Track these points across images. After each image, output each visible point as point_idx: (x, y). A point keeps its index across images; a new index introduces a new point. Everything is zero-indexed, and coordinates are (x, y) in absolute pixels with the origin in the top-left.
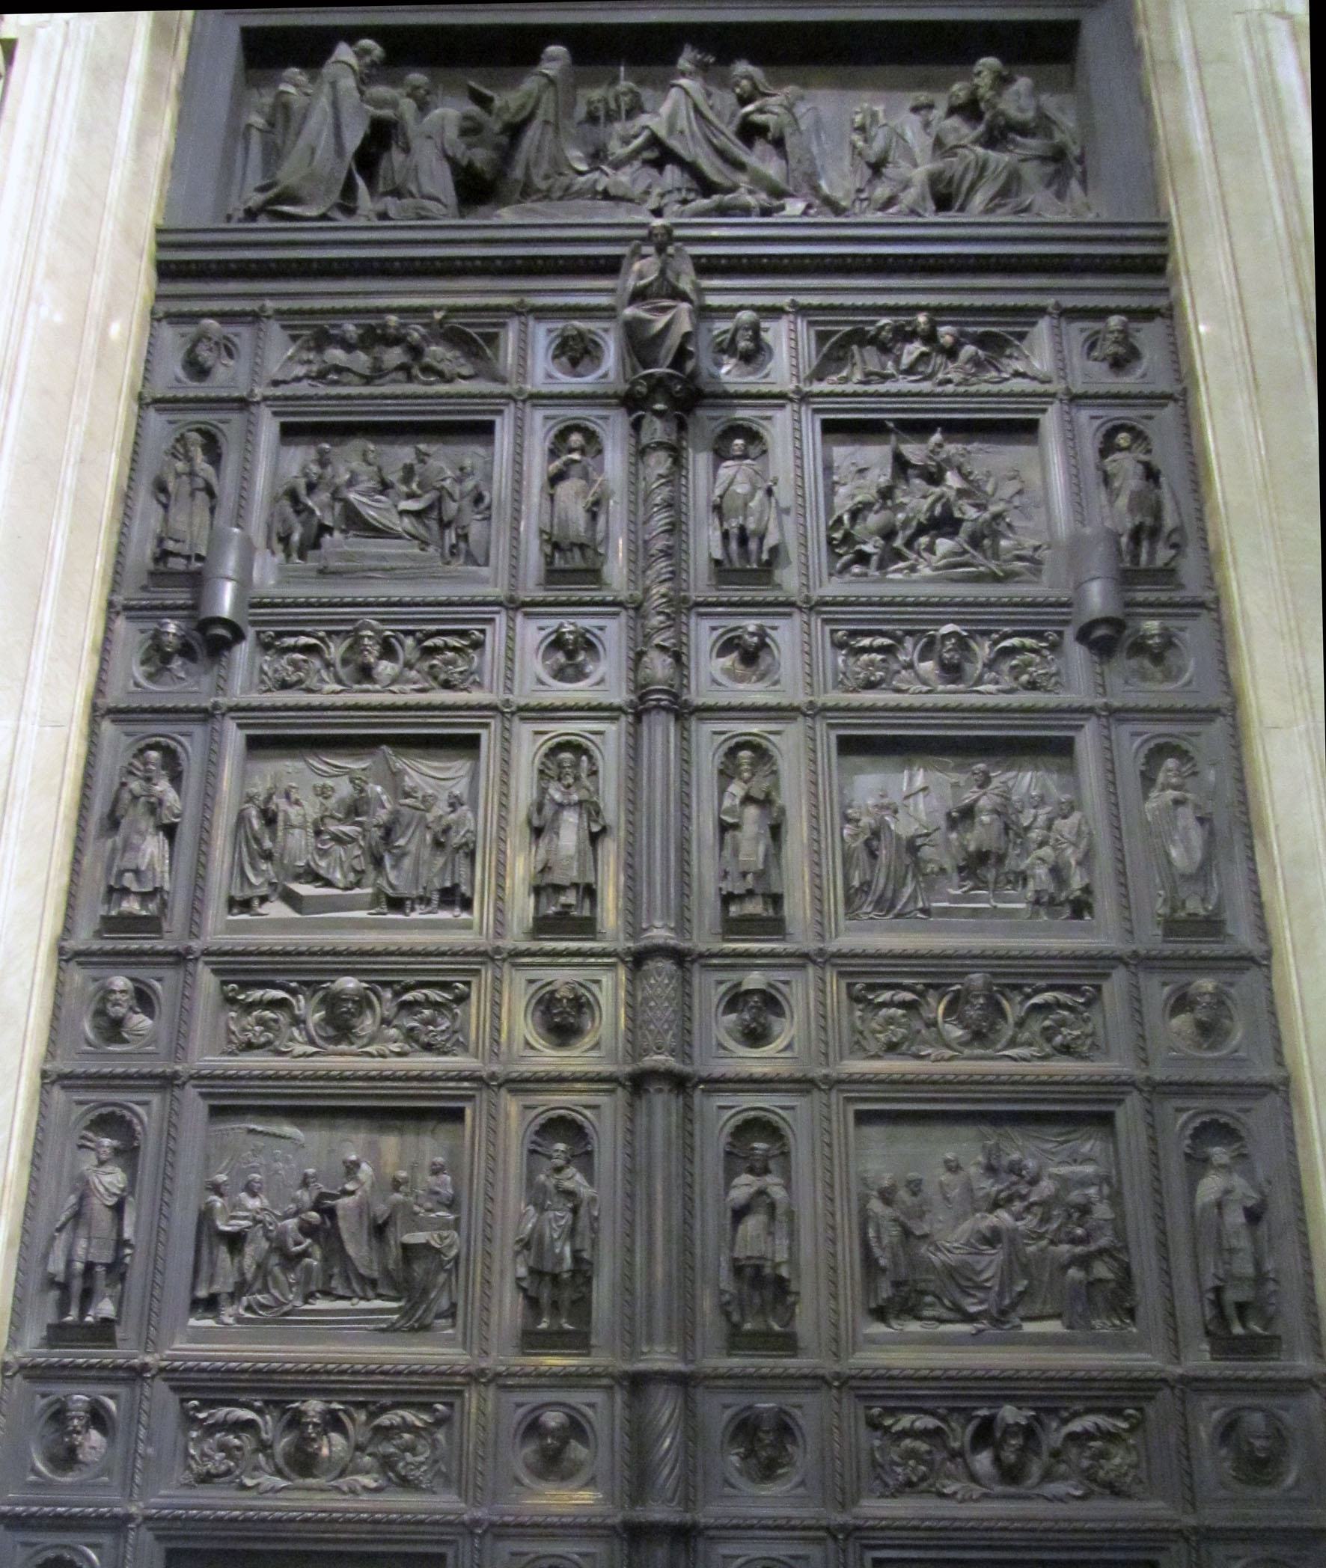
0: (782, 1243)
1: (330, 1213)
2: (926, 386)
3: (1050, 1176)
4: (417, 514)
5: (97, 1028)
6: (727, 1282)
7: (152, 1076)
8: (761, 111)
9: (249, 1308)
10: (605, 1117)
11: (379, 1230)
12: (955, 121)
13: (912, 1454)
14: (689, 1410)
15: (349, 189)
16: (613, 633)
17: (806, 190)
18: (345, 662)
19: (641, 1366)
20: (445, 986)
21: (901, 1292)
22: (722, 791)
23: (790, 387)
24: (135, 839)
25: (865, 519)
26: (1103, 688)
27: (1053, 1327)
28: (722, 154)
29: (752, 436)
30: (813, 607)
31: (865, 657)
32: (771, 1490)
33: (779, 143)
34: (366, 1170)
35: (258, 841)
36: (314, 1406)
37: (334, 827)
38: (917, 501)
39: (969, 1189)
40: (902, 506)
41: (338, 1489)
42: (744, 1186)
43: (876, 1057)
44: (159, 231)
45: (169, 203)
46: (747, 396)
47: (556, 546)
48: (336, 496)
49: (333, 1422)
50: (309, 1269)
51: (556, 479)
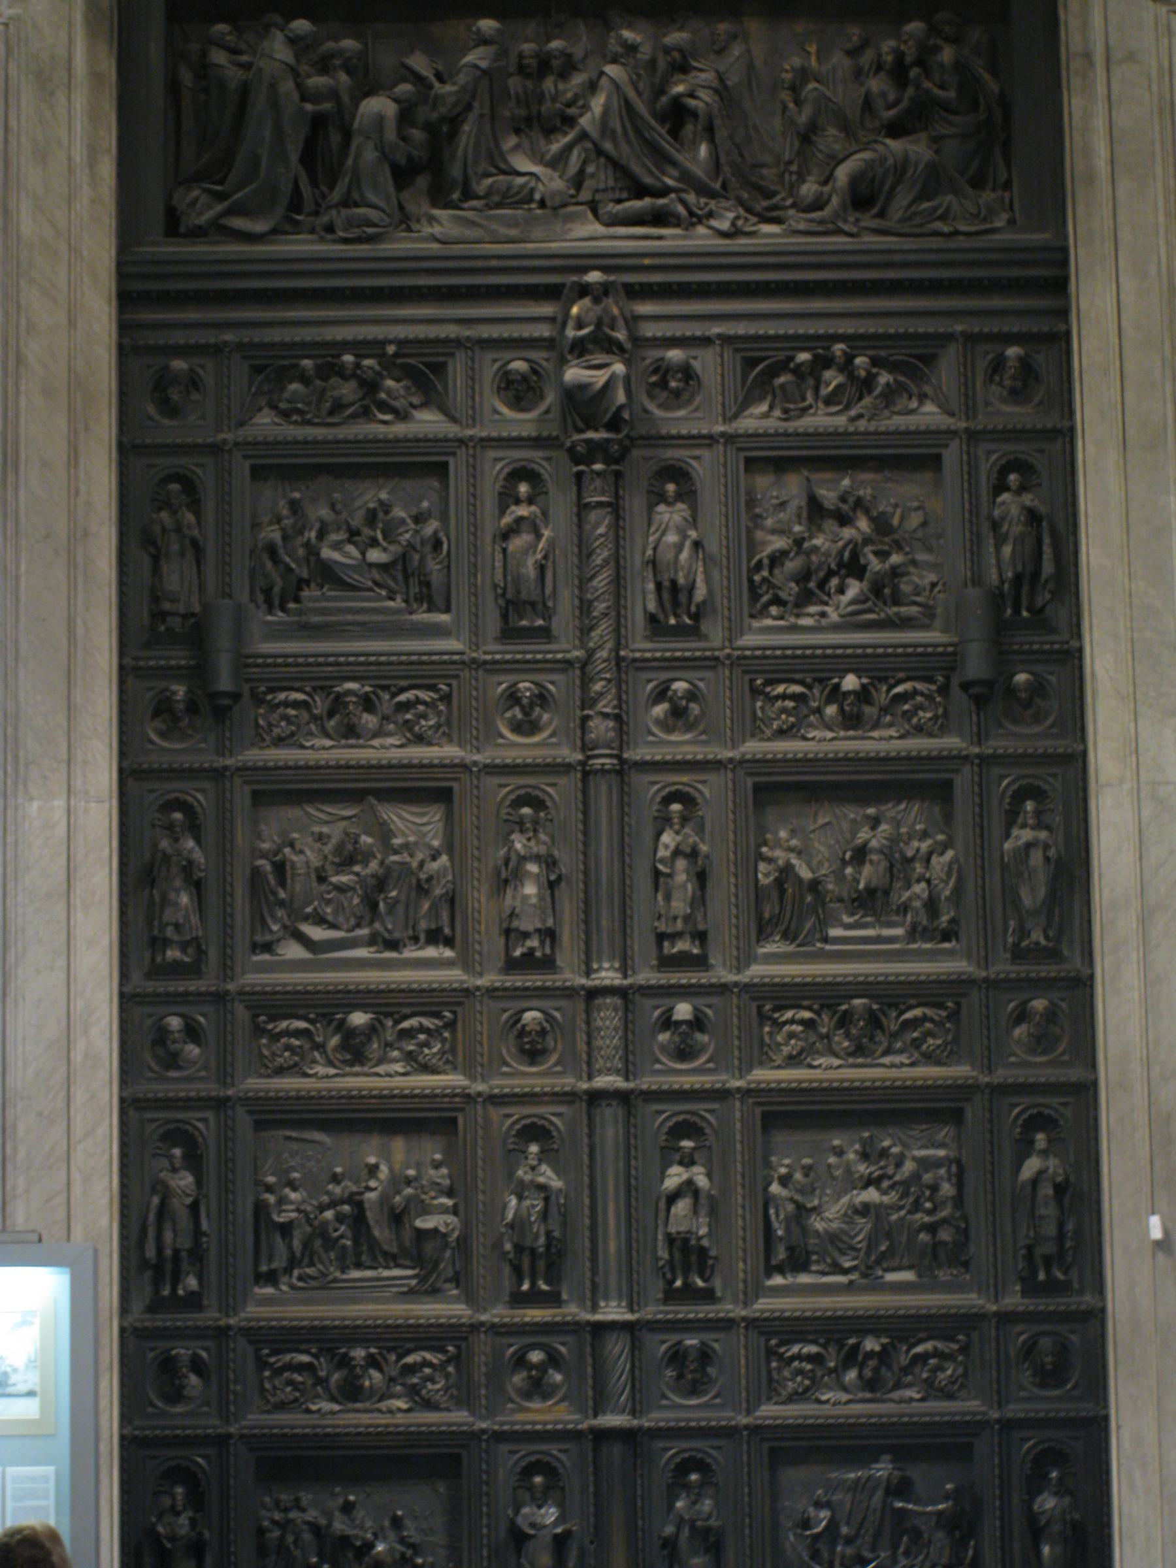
0: (703, 1220)
2: (840, 421)
3: (914, 1159)
4: (383, 567)
6: (663, 1253)
7: (211, 1099)
8: (692, 95)
9: (300, 1278)
13: (800, 1372)
14: (635, 1347)
17: (733, 182)
19: (598, 1317)
22: (659, 834)
24: (172, 896)
25: (783, 565)
27: (907, 1276)
31: (779, 703)
33: (710, 131)
34: (384, 1170)
35: (274, 894)
36: (359, 1353)
38: (826, 542)
41: (380, 1411)
42: (675, 1176)
43: (779, 1067)
46: (680, 437)
47: (508, 602)
49: (372, 1362)
50: (344, 1247)
51: (506, 535)
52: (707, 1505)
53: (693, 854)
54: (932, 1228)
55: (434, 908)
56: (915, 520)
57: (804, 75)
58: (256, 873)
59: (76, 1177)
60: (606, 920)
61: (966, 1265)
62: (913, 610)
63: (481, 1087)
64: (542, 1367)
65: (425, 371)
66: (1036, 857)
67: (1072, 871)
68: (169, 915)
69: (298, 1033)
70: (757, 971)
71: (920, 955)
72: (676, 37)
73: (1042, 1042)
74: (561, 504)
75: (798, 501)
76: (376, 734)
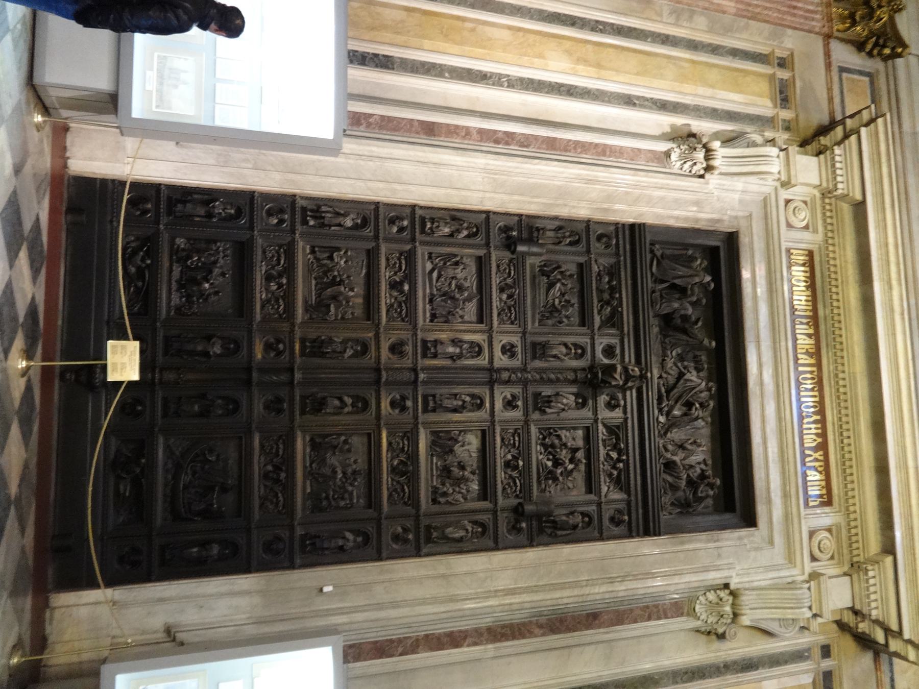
1: (339, 285)
2: (602, 459)
5: (392, 217)
6: (319, 395)
8: (696, 409)
10: (369, 360)
11: (334, 298)
12: (699, 471)
13: (272, 448)
15: (663, 281)
16: (517, 363)
18: (506, 284)
19: (296, 370)
20: (406, 316)
21: (317, 445)
22: (468, 395)
23: (600, 417)
26: (503, 510)
29: (584, 405)
30: (527, 422)
32: (261, 407)
33: (685, 414)
34: (351, 294)
36: (284, 281)
37: (454, 282)
38: (564, 455)
39: (350, 465)
40: (561, 450)
42: (348, 401)
44: (644, 224)
45: (653, 227)
48: (559, 280)
49: (280, 286)
51: (565, 345)
54: (327, 498)
55: (442, 316)
56: (570, 485)
59: (353, 182)
61: (312, 512)
62: (543, 486)
63: (382, 330)
64: (276, 349)
66: (462, 533)
67: (460, 547)
68: (442, 224)
71: (427, 490)
73: (396, 538)
74: (575, 364)
76: (501, 299)
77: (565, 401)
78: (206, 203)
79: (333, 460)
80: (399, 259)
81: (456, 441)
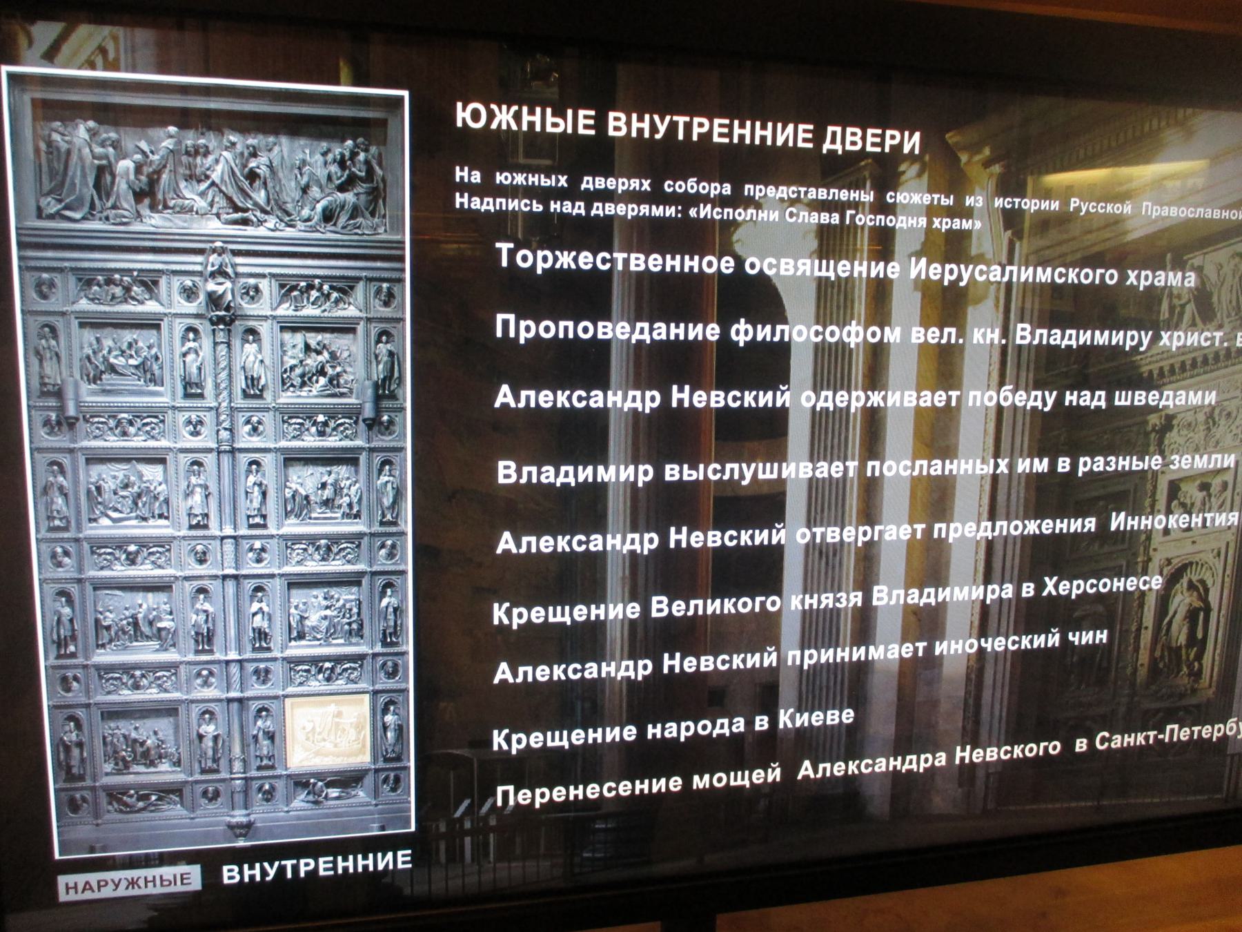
4: (136, 367)
11: (151, 623)
14: (242, 668)
16: (208, 418)
26: (369, 441)
28: (242, 191)
30: (276, 409)
34: (145, 606)
36: (138, 673)
38: (313, 362)
42: (255, 606)
49: (143, 676)
52: (268, 723)
53: (260, 485)
57: (304, 162)
58: (89, 492)
60: (227, 509)
64: (207, 677)
65: (149, 283)
68: (54, 507)
69: (109, 554)
70: (285, 530)
72: (251, 141)
74: (206, 342)
75: (301, 345)
76: (136, 435)
77: (251, 358)
78: (67, 749)
79: (313, 619)
80: (100, 555)
81: (296, 491)
